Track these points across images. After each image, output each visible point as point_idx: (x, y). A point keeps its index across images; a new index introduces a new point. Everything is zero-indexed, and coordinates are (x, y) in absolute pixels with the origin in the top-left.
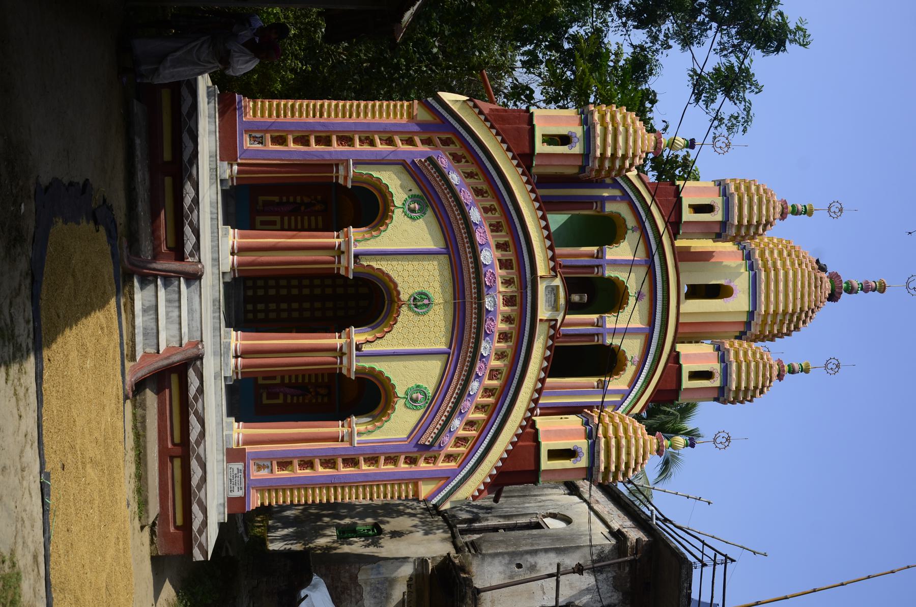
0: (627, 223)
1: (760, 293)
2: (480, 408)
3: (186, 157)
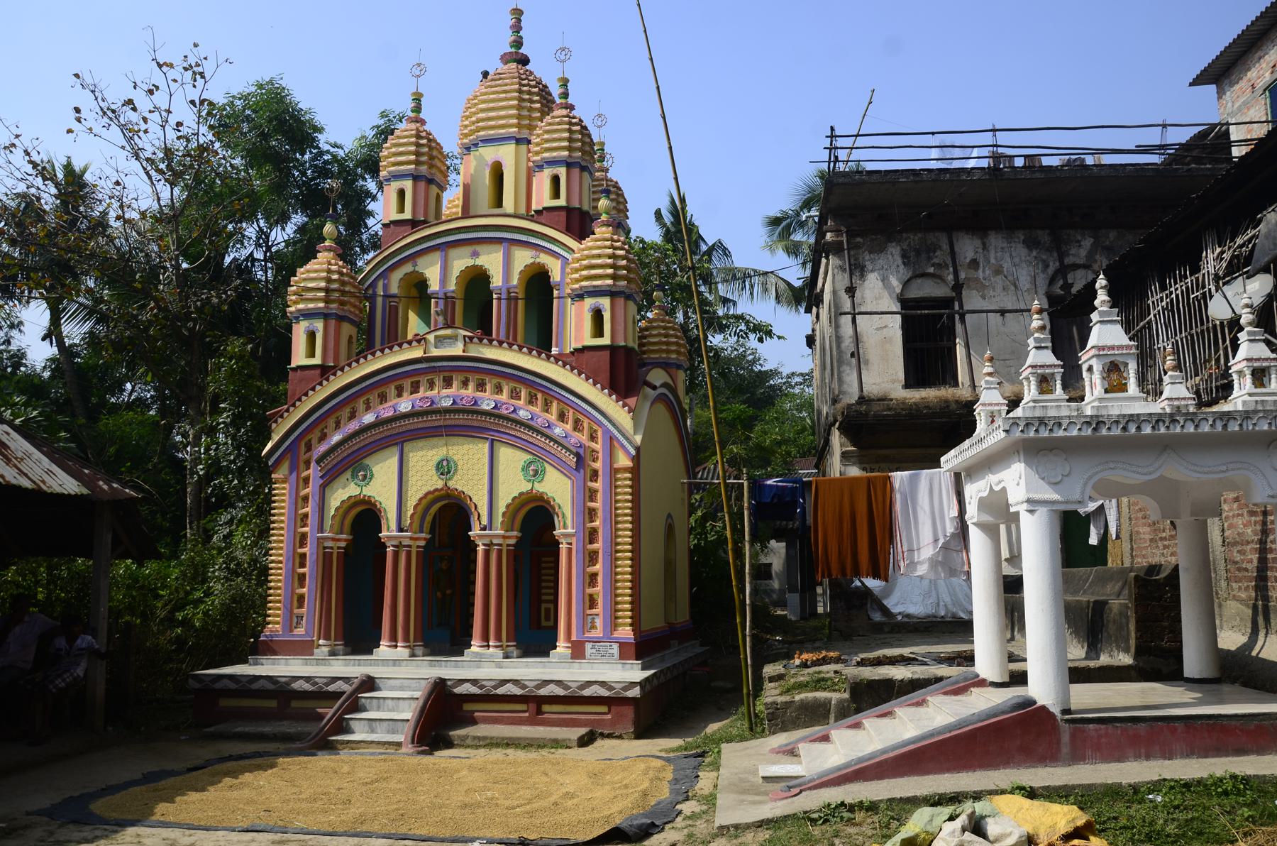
0: (408, 271)
1: (498, 134)
2: (547, 409)
3: (271, 687)
